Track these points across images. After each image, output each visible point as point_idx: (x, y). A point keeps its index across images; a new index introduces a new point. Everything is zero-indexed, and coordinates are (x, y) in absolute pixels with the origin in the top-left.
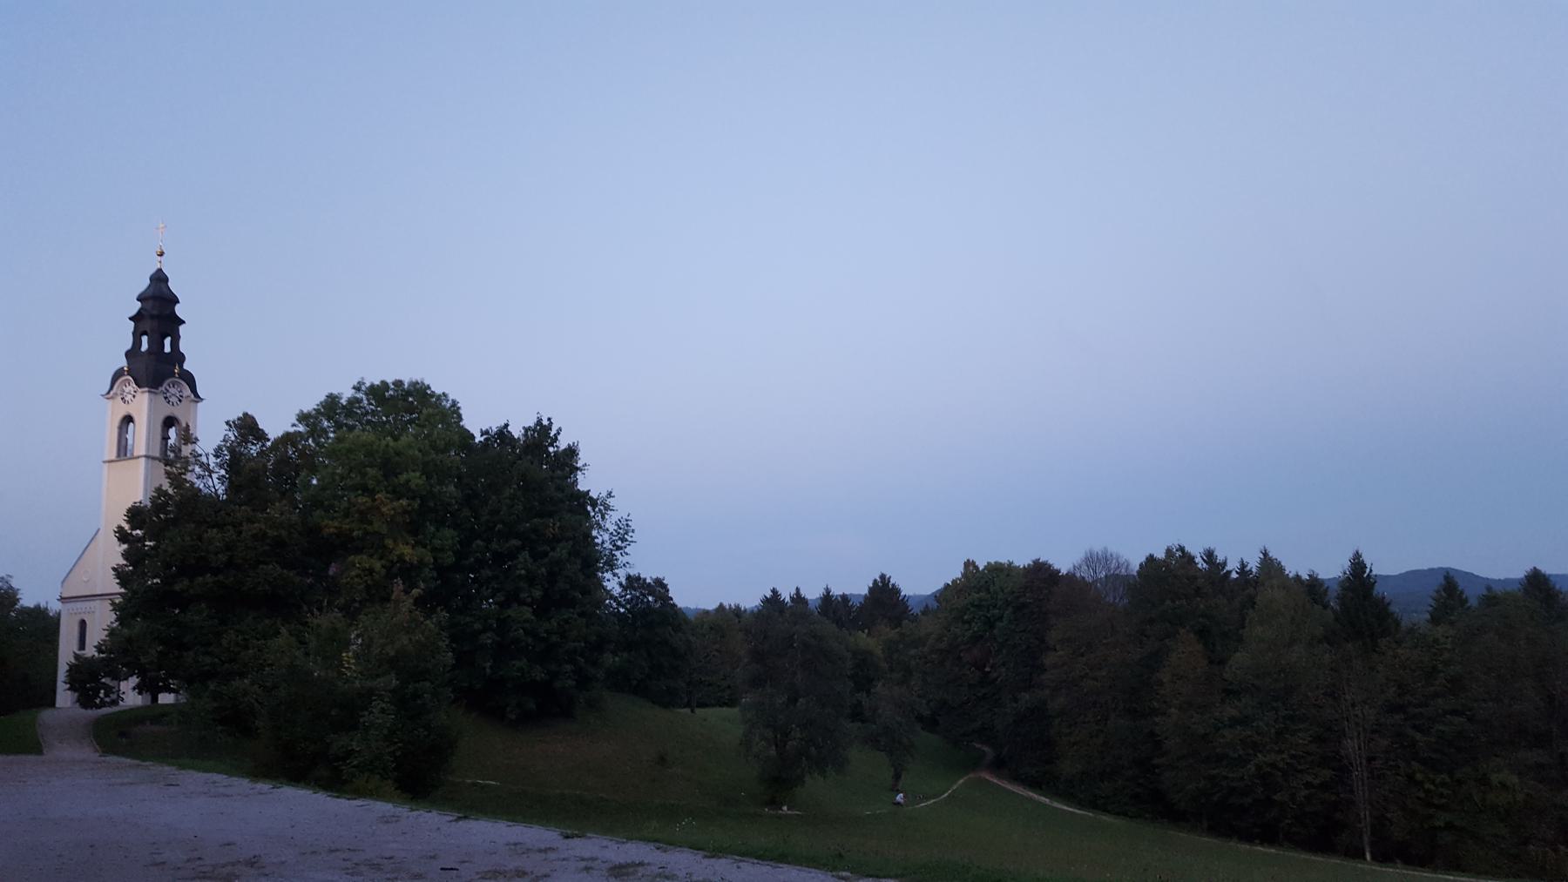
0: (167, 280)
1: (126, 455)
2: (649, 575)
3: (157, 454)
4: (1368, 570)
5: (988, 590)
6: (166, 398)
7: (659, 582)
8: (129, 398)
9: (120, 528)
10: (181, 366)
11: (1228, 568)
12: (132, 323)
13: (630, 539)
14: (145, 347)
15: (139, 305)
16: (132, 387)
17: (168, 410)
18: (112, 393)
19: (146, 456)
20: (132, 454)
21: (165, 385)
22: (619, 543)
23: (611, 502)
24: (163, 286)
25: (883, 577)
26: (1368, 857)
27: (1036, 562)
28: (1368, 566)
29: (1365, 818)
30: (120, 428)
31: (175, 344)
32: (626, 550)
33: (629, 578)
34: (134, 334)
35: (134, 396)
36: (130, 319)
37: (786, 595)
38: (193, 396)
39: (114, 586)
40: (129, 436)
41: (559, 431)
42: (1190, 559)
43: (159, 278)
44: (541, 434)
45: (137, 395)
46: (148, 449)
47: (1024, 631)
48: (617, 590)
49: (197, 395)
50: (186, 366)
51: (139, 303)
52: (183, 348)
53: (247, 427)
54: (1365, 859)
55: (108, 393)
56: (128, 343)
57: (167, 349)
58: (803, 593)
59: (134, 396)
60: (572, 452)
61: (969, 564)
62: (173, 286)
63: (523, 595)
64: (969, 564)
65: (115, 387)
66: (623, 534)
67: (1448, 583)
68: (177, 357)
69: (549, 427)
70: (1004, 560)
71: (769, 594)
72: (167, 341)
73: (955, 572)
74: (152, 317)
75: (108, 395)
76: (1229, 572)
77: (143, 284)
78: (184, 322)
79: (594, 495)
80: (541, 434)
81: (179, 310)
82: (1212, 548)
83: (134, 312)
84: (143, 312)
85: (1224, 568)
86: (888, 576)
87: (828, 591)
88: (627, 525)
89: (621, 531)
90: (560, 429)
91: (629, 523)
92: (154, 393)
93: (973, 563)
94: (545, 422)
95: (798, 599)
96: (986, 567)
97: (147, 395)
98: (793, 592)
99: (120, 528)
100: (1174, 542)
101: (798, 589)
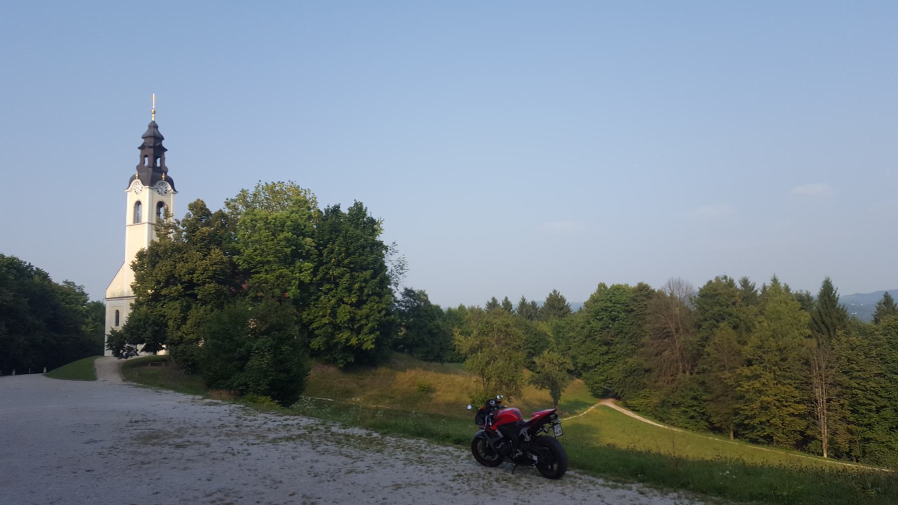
2: (416, 288)
3: (154, 222)
4: (834, 292)
5: (611, 301)
7: (422, 293)
9: (133, 263)
10: (166, 173)
11: (755, 289)
12: (139, 151)
13: (406, 268)
14: (146, 164)
15: (143, 141)
16: (140, 185)
17: (160, 198)
18: (130, 188)
19: (149, 223)
20: (141, 222)
22: (401, 271)
23: (396, 248)
24: (155, 130)
25: (555, 291)
26: (825, 455)
27: (640, 285)
28: (835, 288)
29: (824, 434)
30: (135, 208)
31: (162, 162)
32: (404, 274)
33: (406, 289)
34: (141, 156)
36: (139, 148)
37: (500, 302)
38: (172, 190)
39: (132, 293)
42: (731, 284)
43: (154, 126)
44: (358, 210)
45: (143, 189)
46: (149, 220)
47: (631, 325)
48: (399, 297)
49: (175, 190)
50: (168, 174)
51: (143, 141)
52: (167, 164)
53: (199, 208)
54: (822, 455)
56: (138, 162)
57: (158, 165)
58: (509, 300)
60: (372, 222)
61: (602, 286)
62: (162, 131)
63: (345, 299)
64: (602, 286)
65: (131, 185)
66: (401, 267)
67: (887, 300)
68: (163, 170)
70: (622, 282)
71: (491, 301)
72: (158, 160)
73: (593, 289)
74: (150, 147)
76: (757, 291)
77: (144, 129)
78: (166, 150)
79: (385, 244)
80: (358, 210)
81: (165, 144)
82: (747, 276)
83: (140, 145)
84: (145, 145)
85: (753, 290)
87: (524, 300)
88: (404, 261)
89: (401, 264)
91: (405, 259)
92: (152, 189)
95: (507, 305)
96: (611, 287)
97: (148, 190)
98: (504, 299)
99: (133, 263)
100: (721, 274)
101: (506, 298)
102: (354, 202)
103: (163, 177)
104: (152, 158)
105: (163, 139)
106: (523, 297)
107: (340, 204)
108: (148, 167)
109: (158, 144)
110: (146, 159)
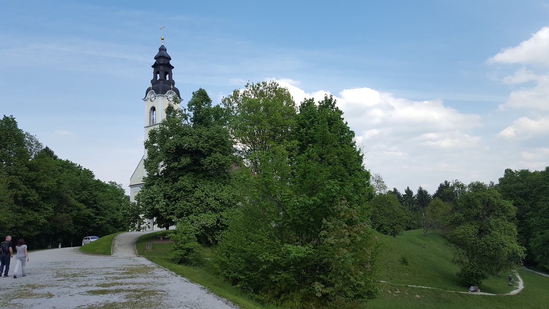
0: (166, 50)
1: (153, 124)
6: (168, 99)
8: (153, 99)
10: (173, 86)
12: (153, 69)
14: (158, 78)
18: (146, 98)
20: (155, 123)
21: (167, 93)
24: (164, 52)
25: (446, 182)
31: (170, 77)
35: (155, 98)
36: (152, 67)
40: (154, 116)
41: (335, 103)
43: (162, 49)
45: (156, 97)
51: (155, 60)
52: (174, 78)
55: (145, 98)
57: (168, 79)
58: (410, 189)
59: (155, 98)
62: (169, 52)
65: (147, 96)
69: (332, 98)
71: (393, 190)
72: (167, 76)
74: (161, 65)
75: (145, 99)
77: (156, 52)
78: (173, 68)
81: (171, 63)
84: (157, 63)
86: (448, 182)
87: (421, 188)
90: (335, 100)
92: (163, 96)
93: (510, 170)
94: (329, 98)
95: (409, 192)
98: (406, 188)
101: (408, 187)
102: (326, 95)
103: (171, 87)
104: (162, 73)
105: (171, 59)
106: (420, 186)
107: (313, 98)
108: (160, 80)
109: (167, 62)
110: (158, 75)
